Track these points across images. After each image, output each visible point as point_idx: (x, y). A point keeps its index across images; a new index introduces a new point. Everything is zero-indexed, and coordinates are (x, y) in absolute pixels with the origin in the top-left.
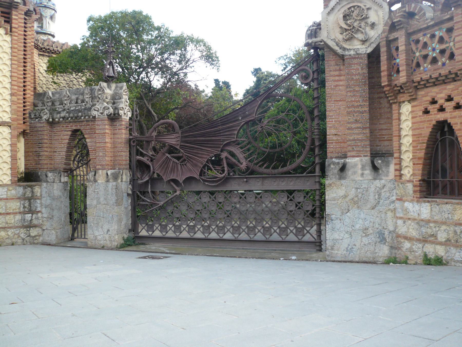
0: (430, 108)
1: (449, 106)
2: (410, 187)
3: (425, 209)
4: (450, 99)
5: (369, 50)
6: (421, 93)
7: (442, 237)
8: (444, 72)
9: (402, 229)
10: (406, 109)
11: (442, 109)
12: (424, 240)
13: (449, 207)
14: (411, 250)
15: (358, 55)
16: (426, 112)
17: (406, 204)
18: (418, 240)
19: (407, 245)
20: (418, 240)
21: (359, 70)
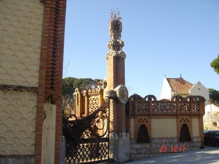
0: (140, 121)
1: (145, 121)
2: (134, 140)
3: (139, 146)
4: (145, 119)
5: (125, 103)
6: (138, 117)
7: (143, 152)
8: (146, 113)
9: (132, 151)
10: (132, 120)
11: (143, 121)
12: (138, 154)
13: (145, 145)
14: (134, 157)
15: (123, 104)
16: (139, 122)
17: (134, 145)
18: (137, 154)
19: (133, 156)
20: (137, 154)
21: (124, 107)
